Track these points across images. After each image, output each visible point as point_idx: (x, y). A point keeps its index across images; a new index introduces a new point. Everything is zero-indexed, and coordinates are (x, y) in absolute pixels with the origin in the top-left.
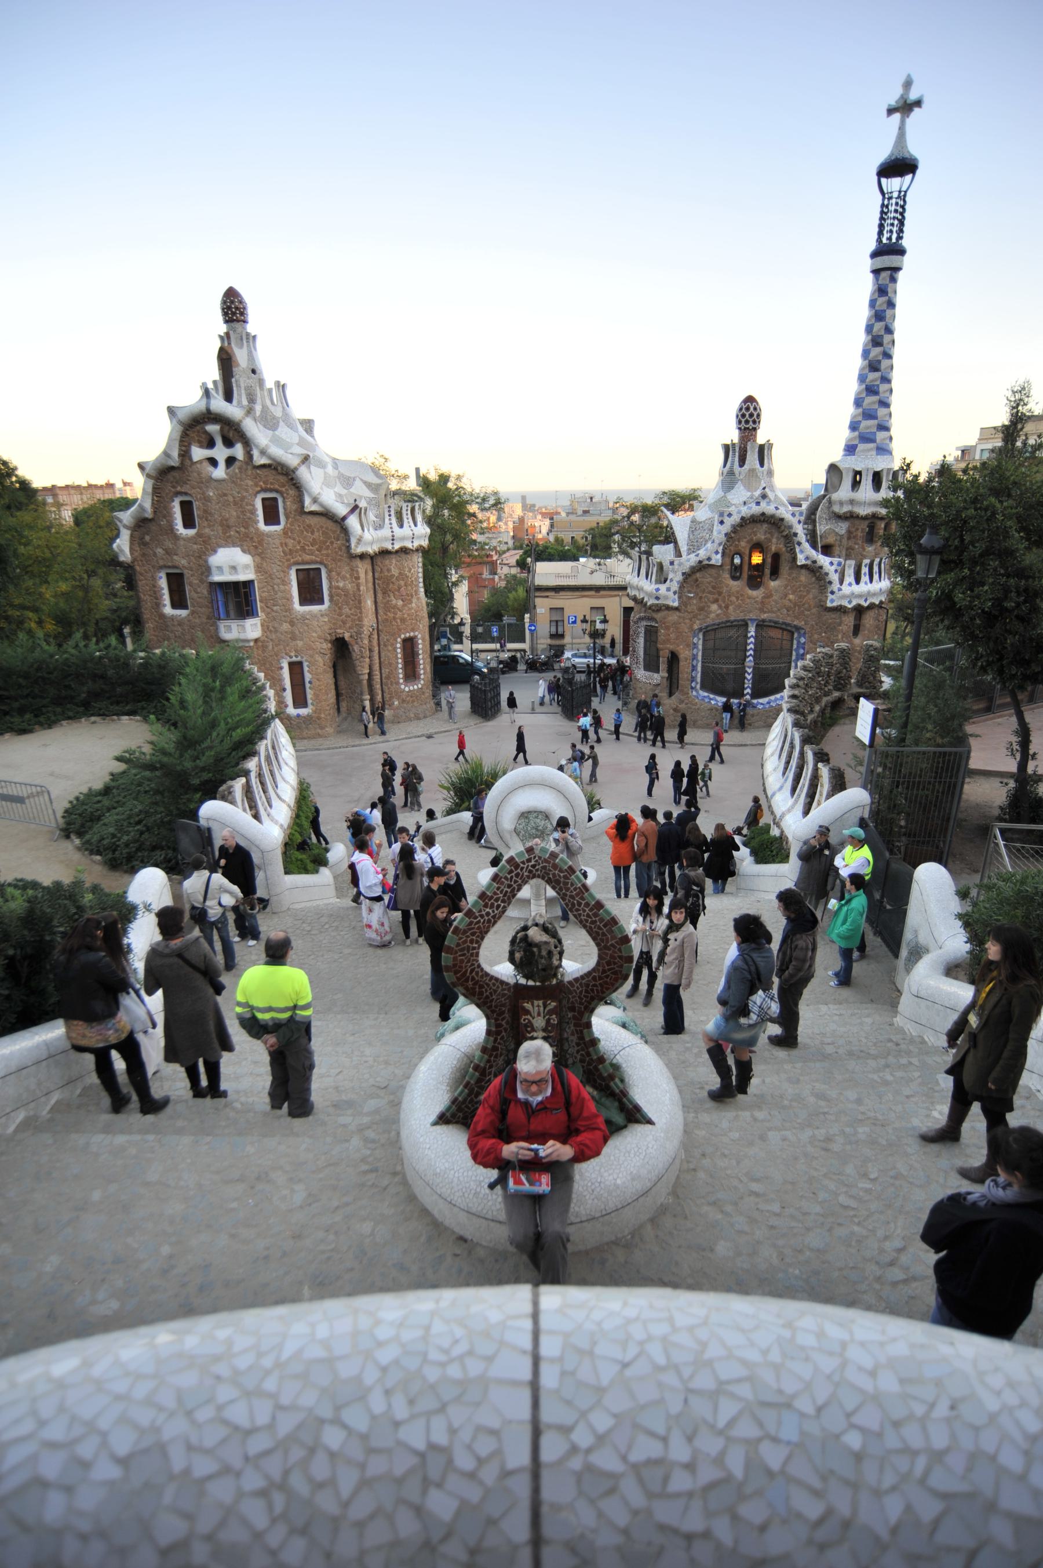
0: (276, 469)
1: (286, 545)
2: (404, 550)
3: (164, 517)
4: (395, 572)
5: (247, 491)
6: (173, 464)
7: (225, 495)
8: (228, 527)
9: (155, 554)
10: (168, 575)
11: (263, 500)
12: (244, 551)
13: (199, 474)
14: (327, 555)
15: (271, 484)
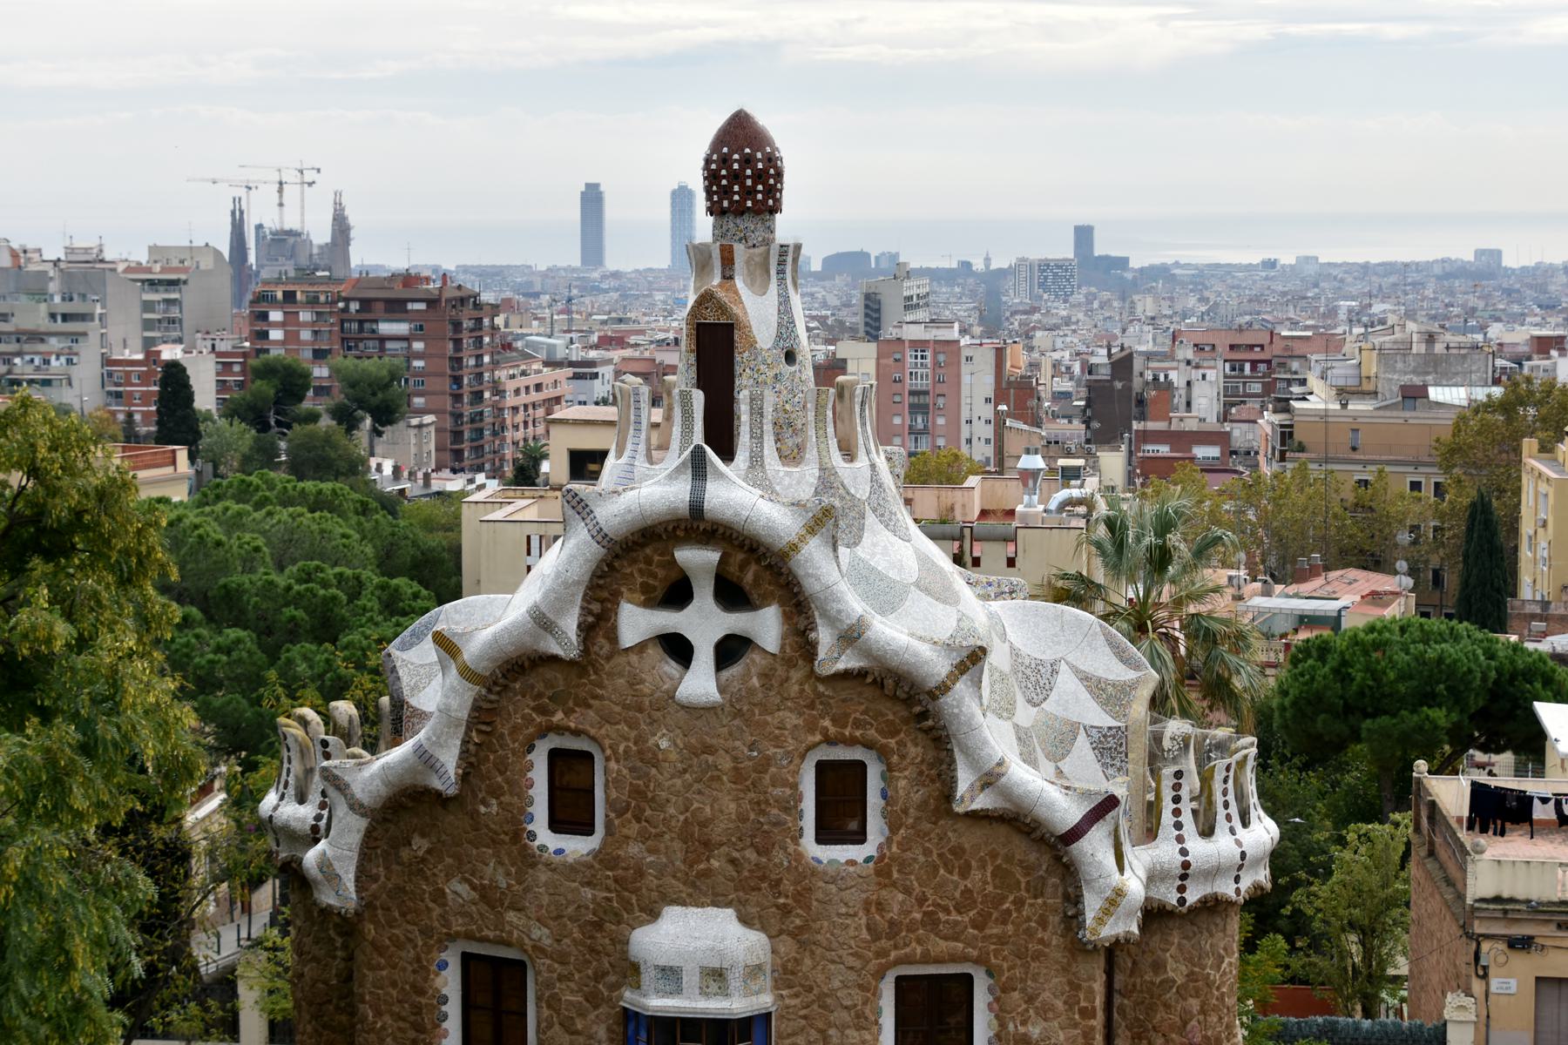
0: (879, 684)
1: (881, 906)
2: (1213, 906)
3: (496, 792)
4: (1176, 971)
5: (778, 741)
6: (556, 649)
7: (709, 749)
8: (707, 844)
9: (444, 893)
10: (467, 960)
11: (821, 767)
12: (745, 920)
13: (634, 682)
14: (1002, 940)
15: (857, 724)
